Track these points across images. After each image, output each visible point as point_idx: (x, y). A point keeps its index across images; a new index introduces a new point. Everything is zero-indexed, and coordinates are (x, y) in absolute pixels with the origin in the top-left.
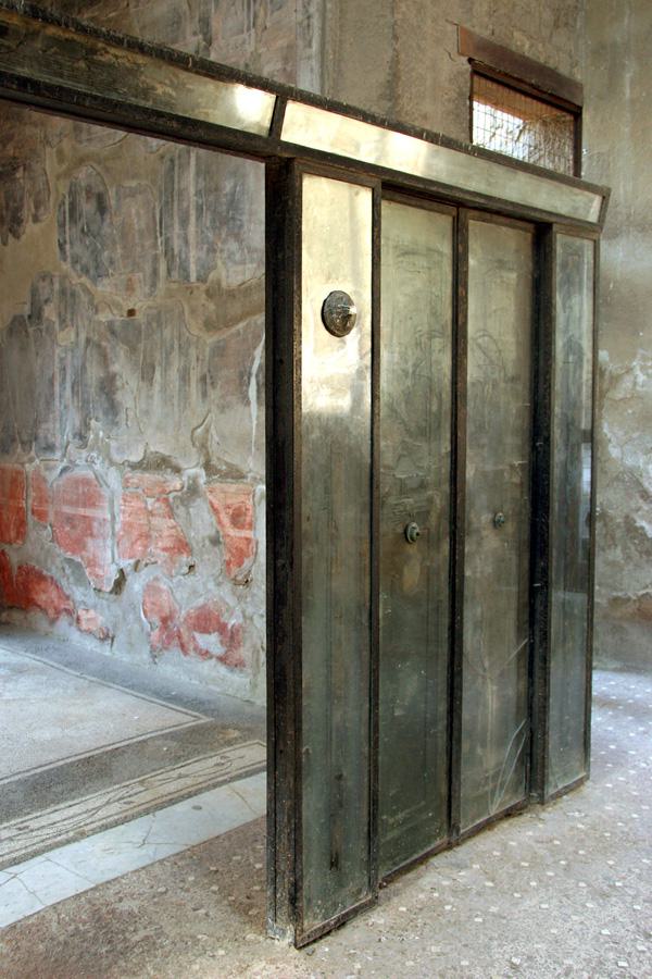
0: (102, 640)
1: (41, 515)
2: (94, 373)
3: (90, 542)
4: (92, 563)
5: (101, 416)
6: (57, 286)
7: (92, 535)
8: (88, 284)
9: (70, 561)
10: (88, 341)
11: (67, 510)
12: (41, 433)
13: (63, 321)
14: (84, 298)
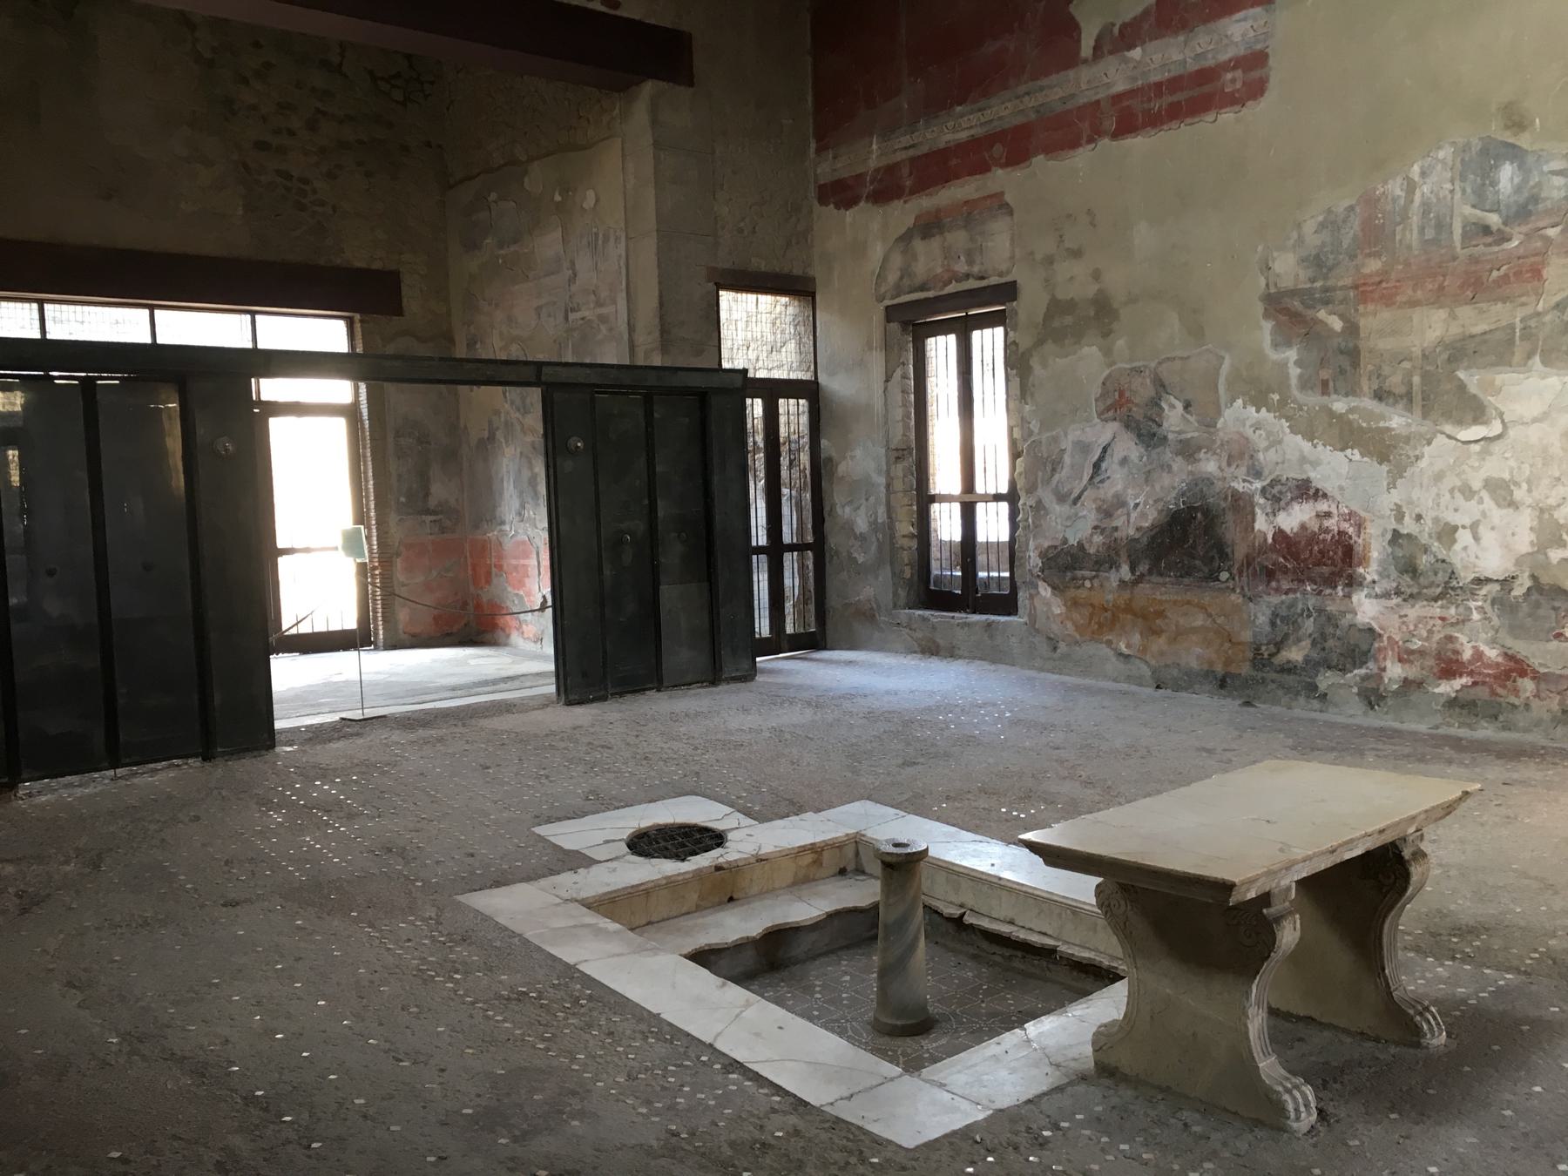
0: (535, 642)
1: (500, 567)
2: (526, 474)
3: (526, 580)
4: (529, 594)
5: (530, 500)
6: (503, 419)
7: (528, 576)
8: (520, 416)
9: (517, 595)
10: (521, 453)
11: (514, 562)
12: (498, 514)
13: (507, 442)
14: (518, 428)
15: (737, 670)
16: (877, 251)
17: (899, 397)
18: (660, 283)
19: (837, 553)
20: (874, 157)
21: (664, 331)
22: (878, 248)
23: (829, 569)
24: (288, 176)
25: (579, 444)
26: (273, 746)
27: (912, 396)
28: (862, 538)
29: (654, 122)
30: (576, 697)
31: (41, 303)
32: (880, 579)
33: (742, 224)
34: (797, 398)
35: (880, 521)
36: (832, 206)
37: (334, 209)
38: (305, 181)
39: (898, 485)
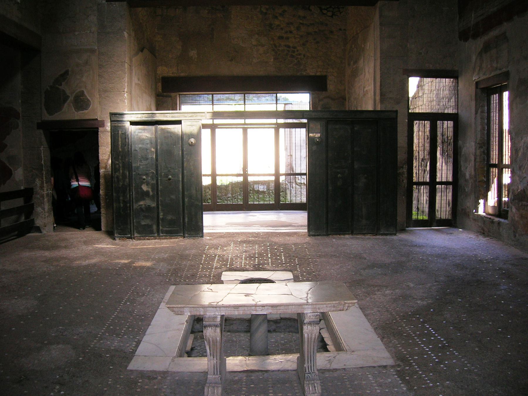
15: (388, 231)
16: (474, 58)
17: (479, 121)
18: (381, 77)
19: (461, 187)
20: (473, 19)
21: (382, 95)
22: (474, 57)
23: (459, 194)
24: (289, 47)
25: (318, 140)
26: (202, 236)
27: (486, 120)
28: (466, 181)
29: (381, 16)
30: (313, 233)
31: (213, 94)
32: (471, 199)
33: (421, 51)
34: (448, 121)
35: (472, 174)
36: (462, 41)
37: (304, 56)
38: (294, 48)
39: (478, 160)
